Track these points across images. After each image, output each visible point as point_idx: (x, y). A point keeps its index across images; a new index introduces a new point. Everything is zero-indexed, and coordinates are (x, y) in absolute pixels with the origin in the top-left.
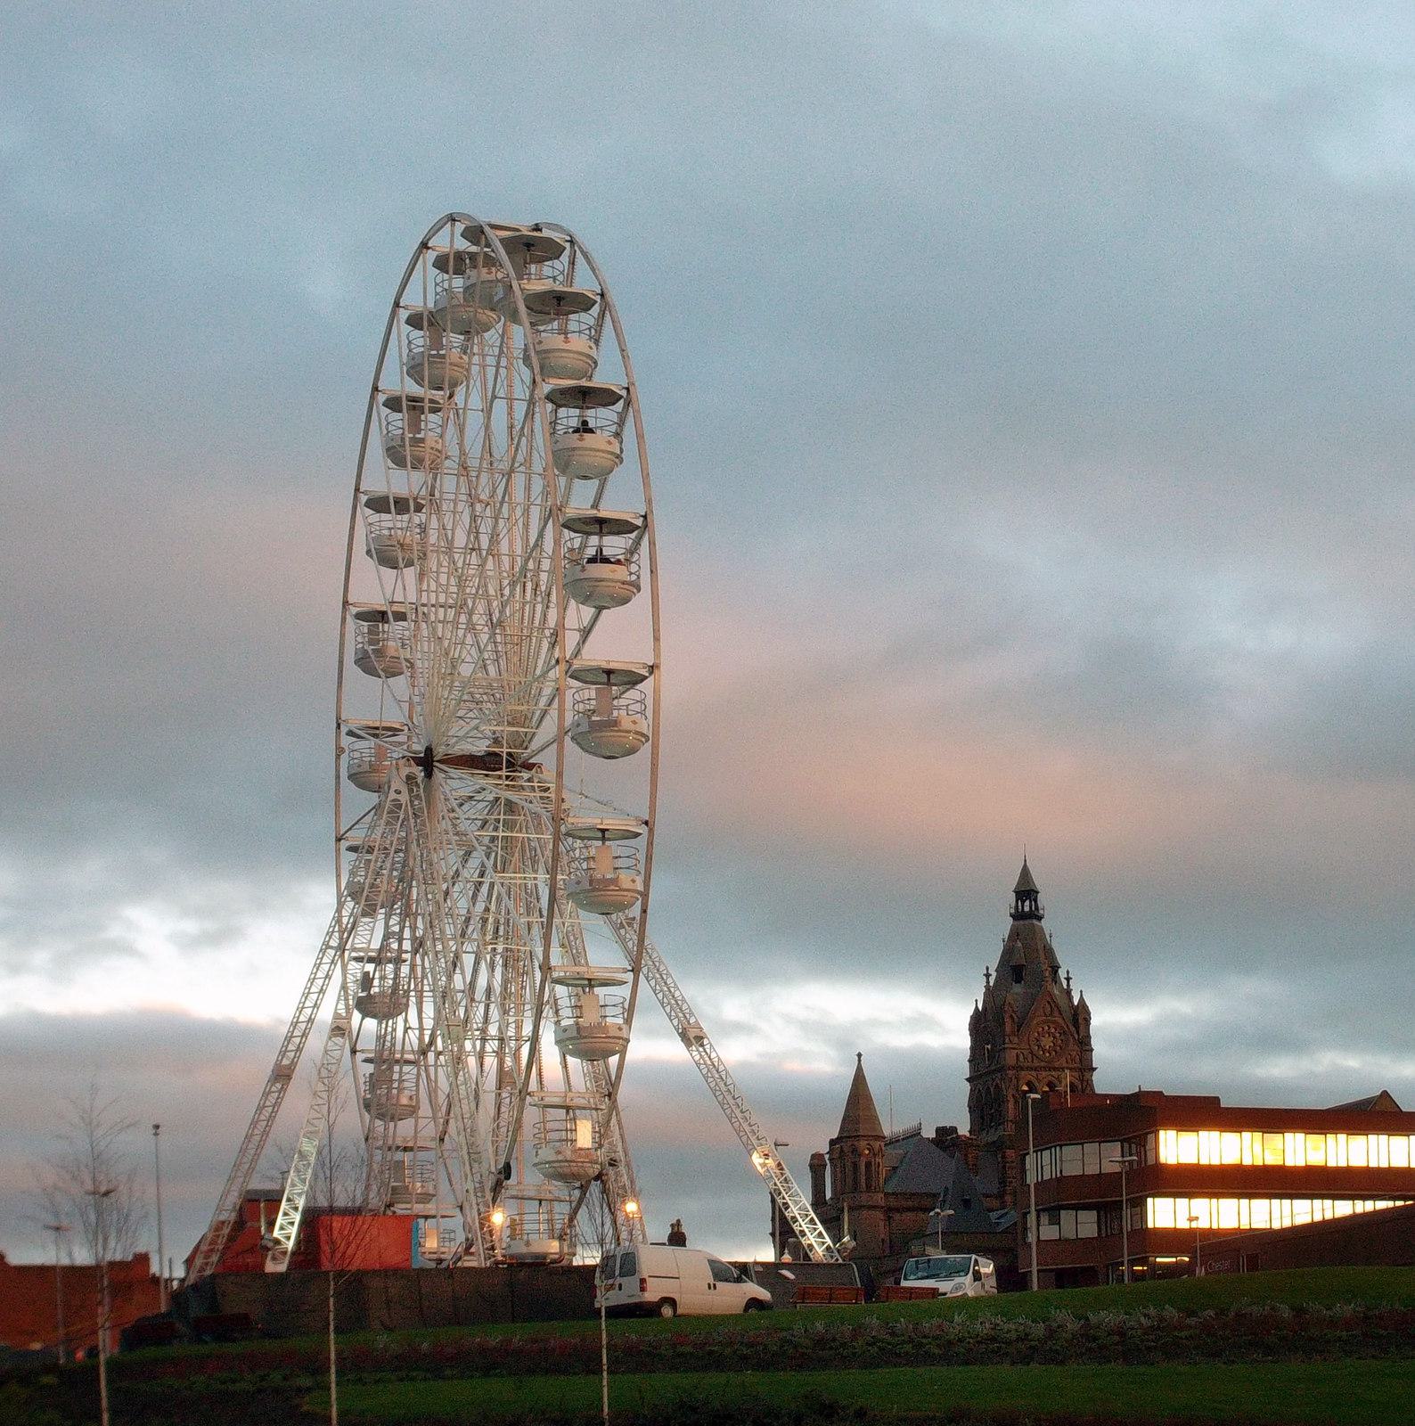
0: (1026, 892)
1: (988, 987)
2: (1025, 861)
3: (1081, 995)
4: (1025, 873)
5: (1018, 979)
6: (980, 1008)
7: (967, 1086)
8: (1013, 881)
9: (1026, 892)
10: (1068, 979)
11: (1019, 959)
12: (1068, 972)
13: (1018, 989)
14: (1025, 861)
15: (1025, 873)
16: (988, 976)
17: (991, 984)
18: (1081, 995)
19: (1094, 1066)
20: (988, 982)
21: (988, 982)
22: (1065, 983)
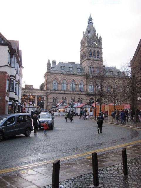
0: (90, 19)
1: (84, 34)
4: (90, 16)
5: (89, 33)
7: (80, 53)
9: (90, 19)
10: (98, 35)
11: (89, 29)
13: (89, 34)
15: (90, 16)
16: (84, 32)
19: (102, 47)
22: (97, 35)
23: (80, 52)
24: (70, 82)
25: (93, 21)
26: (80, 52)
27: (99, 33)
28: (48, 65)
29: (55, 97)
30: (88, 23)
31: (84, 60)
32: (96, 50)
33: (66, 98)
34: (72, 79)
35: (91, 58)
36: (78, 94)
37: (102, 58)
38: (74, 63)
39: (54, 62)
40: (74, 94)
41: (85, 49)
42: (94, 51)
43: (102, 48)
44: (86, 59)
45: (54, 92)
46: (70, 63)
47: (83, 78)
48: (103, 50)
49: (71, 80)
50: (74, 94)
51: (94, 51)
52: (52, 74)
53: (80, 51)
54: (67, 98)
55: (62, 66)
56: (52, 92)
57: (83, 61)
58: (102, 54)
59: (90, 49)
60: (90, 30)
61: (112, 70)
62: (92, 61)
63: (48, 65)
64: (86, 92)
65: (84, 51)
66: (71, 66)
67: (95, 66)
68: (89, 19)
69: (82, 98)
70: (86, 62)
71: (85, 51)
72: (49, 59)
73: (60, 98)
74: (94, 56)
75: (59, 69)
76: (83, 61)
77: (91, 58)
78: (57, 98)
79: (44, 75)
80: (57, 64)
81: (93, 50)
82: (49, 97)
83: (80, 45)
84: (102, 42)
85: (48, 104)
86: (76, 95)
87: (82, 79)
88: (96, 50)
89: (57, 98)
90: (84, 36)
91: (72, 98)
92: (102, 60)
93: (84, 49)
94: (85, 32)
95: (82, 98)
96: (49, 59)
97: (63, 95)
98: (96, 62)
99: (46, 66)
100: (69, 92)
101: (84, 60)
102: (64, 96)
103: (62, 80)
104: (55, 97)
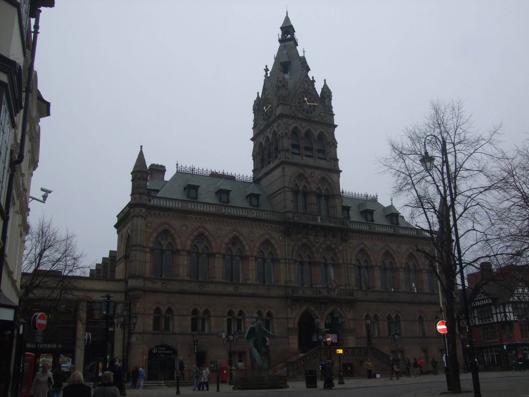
0: (287, 30)
1: (266, 76)
2: (287, 14)
3: (325, 82)
4: (287, 19)
6: (260, 96)
7: (252, 144)
8: (281, 23)
9: (287, 30)
11: (285, 59)
12: (313, 77)
13: (287, 76)
14: (287, 14)
15: (287, 19)
16: (266, 70)
17: (269, 75)
18: (325, 82)
19: (335, 123)
20: (267, 74)
21: (267, 74)
23: (252, 139)
24: (223, 246)
25: (297, 35)
26: (252, 139)
27: (318, 75)
28: (139, 175)
29: (164, 309)
30: (280, 41)
31: (271, 166)
32: (316, 131)
33: (206, 312)
34: (230, 236)
35: (297, 159)
36: (253, 296)
37: (337, 160)
38: (231, 178)
39: (160, 170)
40: (240, 296)
41: (275, 127)
42: (308, 134)
43: (336, 126)
44: (276, 162)
45: (158, 285)
46: (214, 175)
48: (338, 134)
49: (226, 240)
50: (240, 296)
51: (308, 134)
53: (252, 136)
54: (212, 314)
55: (190, 183)
56: (149, 285)
57: (264, 171)
58: (334, 144)
59: (291, 128)
60: (289, 62)
61: (369, 207)
62: (301, 171)
63: (139, 175)
64: (286, 287)
65: (269, 133)
66: (224, 185)
67: (314, 187)
68: (282, 28)
69: (269, 314)
70: (279, 171)
71: (275, 133)
72: (141, 155)
74: (310, 153)
75: (178, 194)
76: (264, 171)
77: (297, 159)
78: (169, 310)
79: (115, 221)
80: (168, 176)
81: (303, 131)
82: (138, 305)
83: (251, 117)
84: (333, 105)
85: (134, 339)
88: (316, 131)
89: (169, 310)
90: (267, 79)
91: (230, 313)
92: (337, 165)
93: (267, 126)
94: (270, 68)
95: (272, 311)
98: (318, 172)
99: (130, 177)
100: (220, 288)
101: (271, 166)
103: (192, 237)
104: (164, 309)
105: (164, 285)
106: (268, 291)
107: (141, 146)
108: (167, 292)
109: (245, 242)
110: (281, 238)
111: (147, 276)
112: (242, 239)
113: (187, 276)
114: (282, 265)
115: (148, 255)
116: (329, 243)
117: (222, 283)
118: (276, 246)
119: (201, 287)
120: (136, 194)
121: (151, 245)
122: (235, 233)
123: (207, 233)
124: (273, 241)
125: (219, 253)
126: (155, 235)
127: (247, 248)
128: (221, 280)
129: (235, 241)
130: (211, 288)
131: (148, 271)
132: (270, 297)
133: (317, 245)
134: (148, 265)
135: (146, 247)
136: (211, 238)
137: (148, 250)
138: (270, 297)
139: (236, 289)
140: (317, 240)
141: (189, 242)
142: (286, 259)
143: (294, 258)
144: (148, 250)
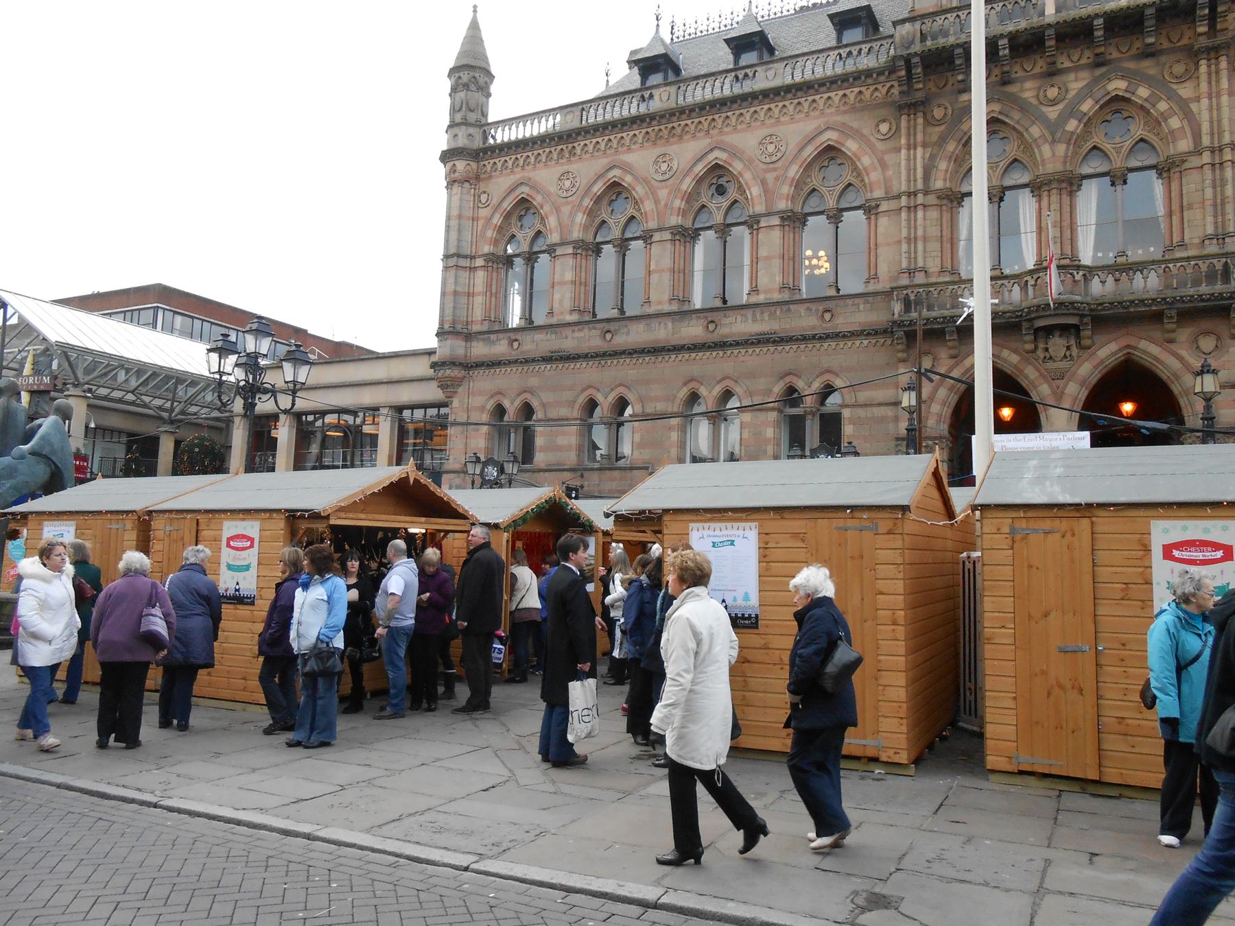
24: (678, 203)
40: (721, 345)
47: (861, 107)
49: (687, 184)
50: (721, 345)
52: (489, 164)
63: (465, 76)
72: (474, 26)
73: (564, 412)
86: (751, 359)
87: (831, 137)
96: (474, 26)
97: (587, 373)
100: (662, 333)
102: (604, 381)
103: (587, 202)
105: (516, 345)
106: (827, 316)
107: (475, 7)
108: (527, 361)
109: (748, 176)
110: (884, 128)
111: (476, 328)
112: (737, 167)
113: (572, 311)
114: (883, 221)
115: (481, 276)
116: (1118, 86)
117: (669, 314)
118: (866, 161)
119: (608, 336)
120: (458, 125)
121: (487, 249)
122: (716, 153)
123: (628, 179)
124: (851, 146)
125: (660, 230)
126: (497, 220)
127: (755, 191)
128: (666, 308)
129: (717, 177)
130: (636, 335)
131: (478, 314)
132: (827, 337)
133: (1052, 113)
134: (479, 300)
135: (473, 258)
136: (639, 191)
137: (479, 262)
138: (827, 337)
139: (711, 327)
140: (1052, 93)
141: (580, 218)
142: (898, 197)
143: (939, 184)
144: (479, 262)
